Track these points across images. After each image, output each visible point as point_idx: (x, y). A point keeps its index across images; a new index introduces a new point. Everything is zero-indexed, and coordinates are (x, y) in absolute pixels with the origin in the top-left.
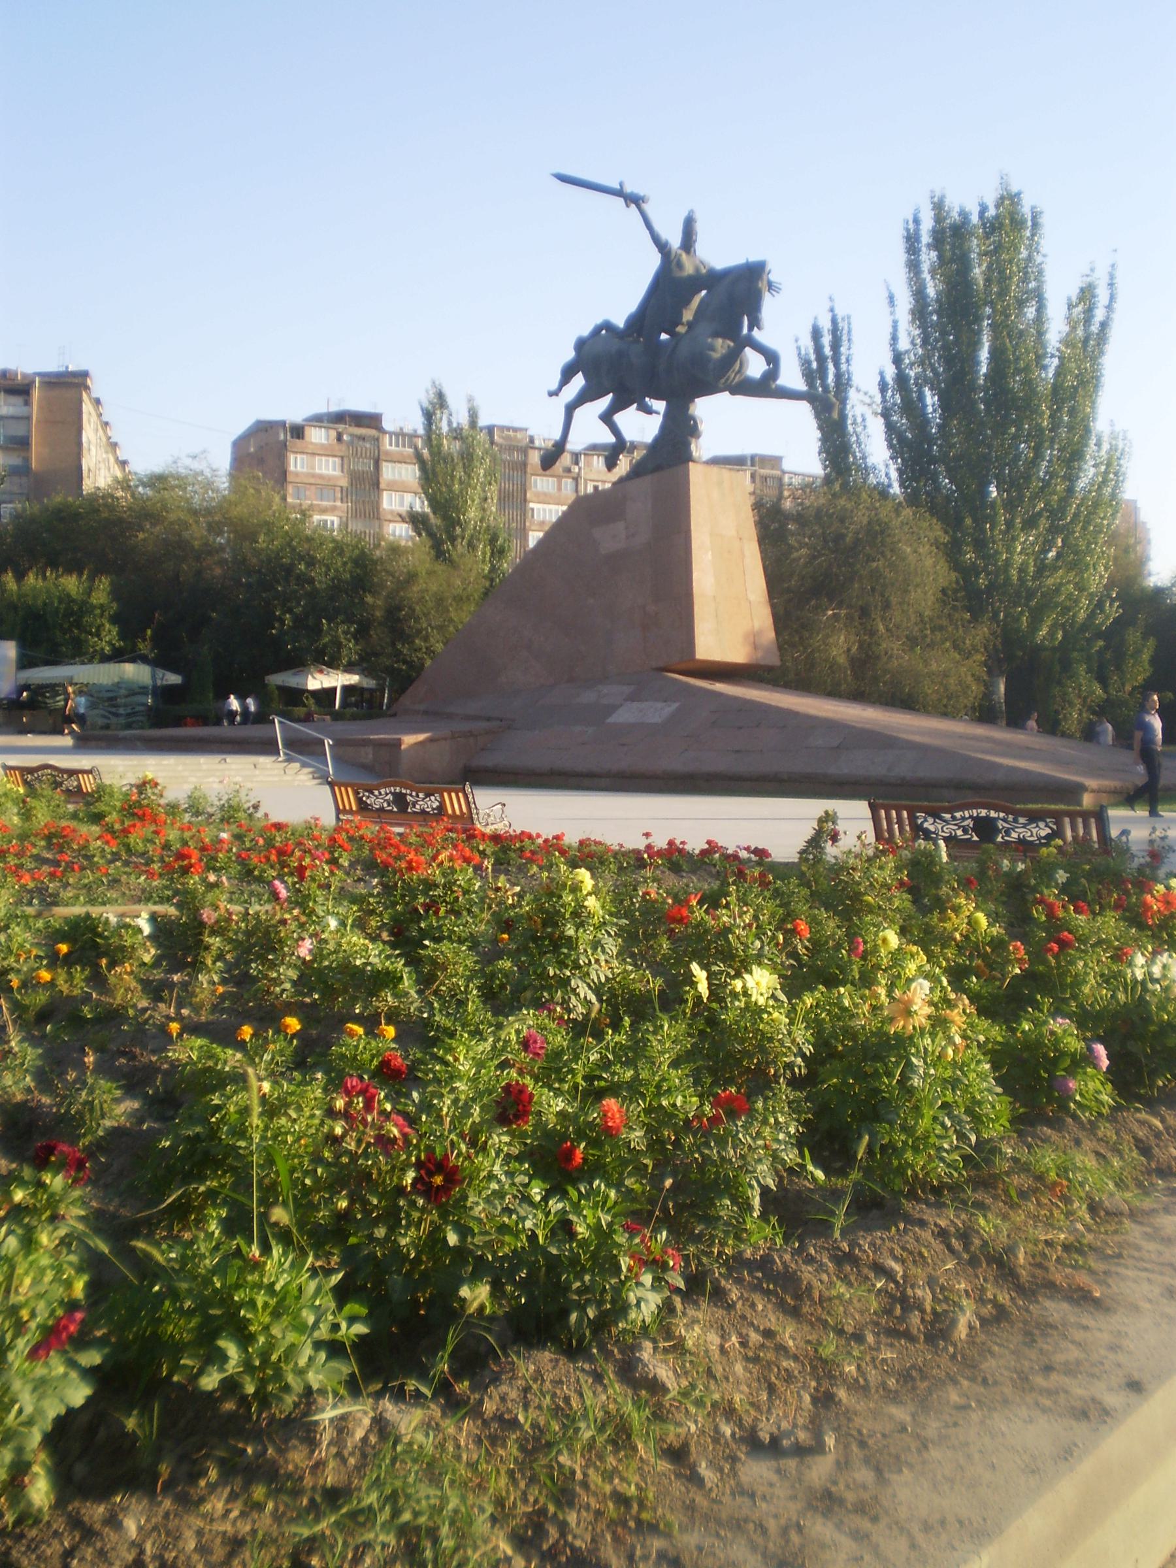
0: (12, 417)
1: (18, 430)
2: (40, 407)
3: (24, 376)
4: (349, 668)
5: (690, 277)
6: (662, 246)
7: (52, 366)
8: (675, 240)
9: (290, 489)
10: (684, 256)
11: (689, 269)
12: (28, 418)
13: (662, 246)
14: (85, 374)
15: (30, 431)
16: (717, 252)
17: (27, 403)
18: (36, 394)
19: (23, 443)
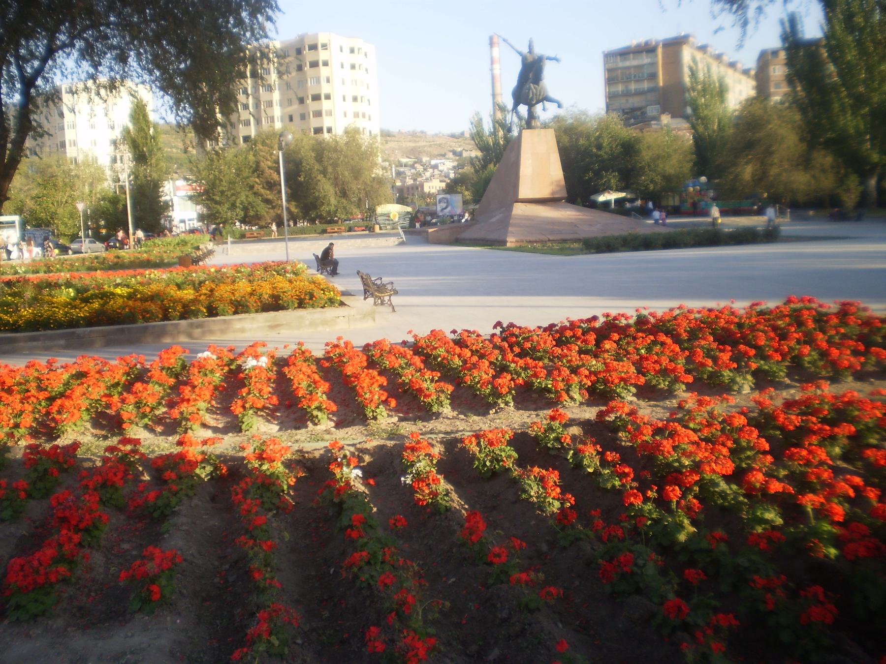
2: (663, 57)
6: (520, 54)
8: (525, 50)
9: (772, 85)
10: (528, 55)
11: (530, 59)
13: (520, 54)
16: (538, 51)
17: (656, 56)
18: (660, 51)
19: (653, 76)
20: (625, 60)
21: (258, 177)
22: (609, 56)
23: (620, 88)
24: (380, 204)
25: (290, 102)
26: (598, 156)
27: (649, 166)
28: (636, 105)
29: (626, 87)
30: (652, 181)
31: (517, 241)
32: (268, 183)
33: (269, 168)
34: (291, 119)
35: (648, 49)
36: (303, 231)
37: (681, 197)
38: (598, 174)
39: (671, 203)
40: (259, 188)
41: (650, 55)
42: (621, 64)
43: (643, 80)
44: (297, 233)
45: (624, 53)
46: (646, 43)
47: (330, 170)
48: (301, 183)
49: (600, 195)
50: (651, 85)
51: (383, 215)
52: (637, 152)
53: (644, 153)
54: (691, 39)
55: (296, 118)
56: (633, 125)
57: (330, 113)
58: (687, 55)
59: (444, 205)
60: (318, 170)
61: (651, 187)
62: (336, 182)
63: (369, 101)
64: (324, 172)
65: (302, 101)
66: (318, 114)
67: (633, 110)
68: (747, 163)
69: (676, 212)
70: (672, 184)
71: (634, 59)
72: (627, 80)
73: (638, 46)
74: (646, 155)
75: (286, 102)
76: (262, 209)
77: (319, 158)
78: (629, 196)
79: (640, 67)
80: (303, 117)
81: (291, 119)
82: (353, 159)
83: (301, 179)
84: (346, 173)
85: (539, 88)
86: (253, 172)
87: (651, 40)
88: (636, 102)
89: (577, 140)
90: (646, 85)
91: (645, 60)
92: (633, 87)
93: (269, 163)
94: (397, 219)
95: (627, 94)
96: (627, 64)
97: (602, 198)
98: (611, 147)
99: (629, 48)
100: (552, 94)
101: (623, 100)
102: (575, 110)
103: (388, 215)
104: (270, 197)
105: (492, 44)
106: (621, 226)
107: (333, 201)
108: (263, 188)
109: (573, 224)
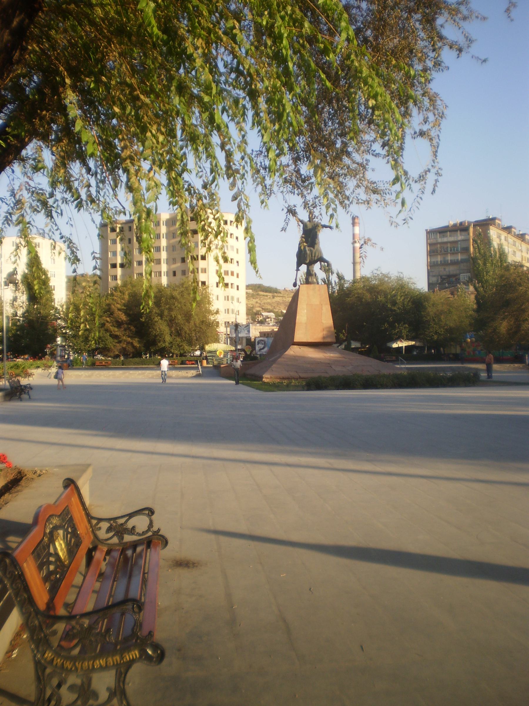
0: (463, 240)
1: (464, 245)
3: (468, 222)
4: (408, 339)
5: (310, 229)
6: (302, 222)
7: (482, 217)
11: (310, 226)
12: (468, 240)
14: (494, 219)
15: (469, 245)
17: (469, 234)
18: (471, 230)
20: (444, 236)
21: (109, 317)
22: (430, 233)
23: (439, 259)
24: (207, 343)
25: (174, 261)
26: (392, 310)
27: (434, 320)
28: (451, 273)
29: (444, 258)
30: (436, 333)
31: (271, 378)
32: (117, 322)
33: (119, 310)
34: (174, 274)
35: (462, 228)
36: (143, 363)
37: (461, 346)
38: (392, 325)
39: (453, 351)
40: (108, 325)
41: (463, 233)
42: (440, 240)
43: (457, 253)
44: (138, 364)
45: (443, 231)
46: (461, 224)
47: (166, 313)
48: (142, 324)
49: (394, 343)
50: (465, 257)
51: (210, 352)
52: (425, 308)
53: (429, 309)
54: (497, 221)
55: (179, 273)
56: (446, 288)
57: (204, 271)
58: (493, 232)
59: (262, 346)
60: (156, 313)
61: (436, 337)
62: (171, 322)
63: (238, 262)
64: (161, 315)
65: (183, 260)
66: (195, 271)
67: (449, 276)
68: (503, 319)
69: (456, 358)
70: (454, 336)
71: (450, 236)
72: (446, 253)
73: (455, 225)
74: (431, 311)
75: (170, 261)
76: (110, 343)
77: (157, 303)
78: (418, 344)
79: (456, 242)
80: (184, 273)
81: (174, 274)
82: (185, 305)
83: (143, 320)
84: (179, 317)
85: (314, 251)
86: (105, 312)
87: (465, 222)
88: (452, 270)
89: (377, 297)
90: (459, 257)
91: (460, 237)
92: (449, 258)
93: (119, 306)
94: (222, 356)
95: (445, 264)
96: (445, 240)
97: (395, 345)
98: (404, 304)
99: (448, 227)
100: (325, 257)
101: (441, 269)
102: (379, 273)
103: (215, 352)
104: (118, 333)
105: (354, 224)
106: (403, 368)
107: (168, 338)
108: (113, 326)
109: (329, 364)
